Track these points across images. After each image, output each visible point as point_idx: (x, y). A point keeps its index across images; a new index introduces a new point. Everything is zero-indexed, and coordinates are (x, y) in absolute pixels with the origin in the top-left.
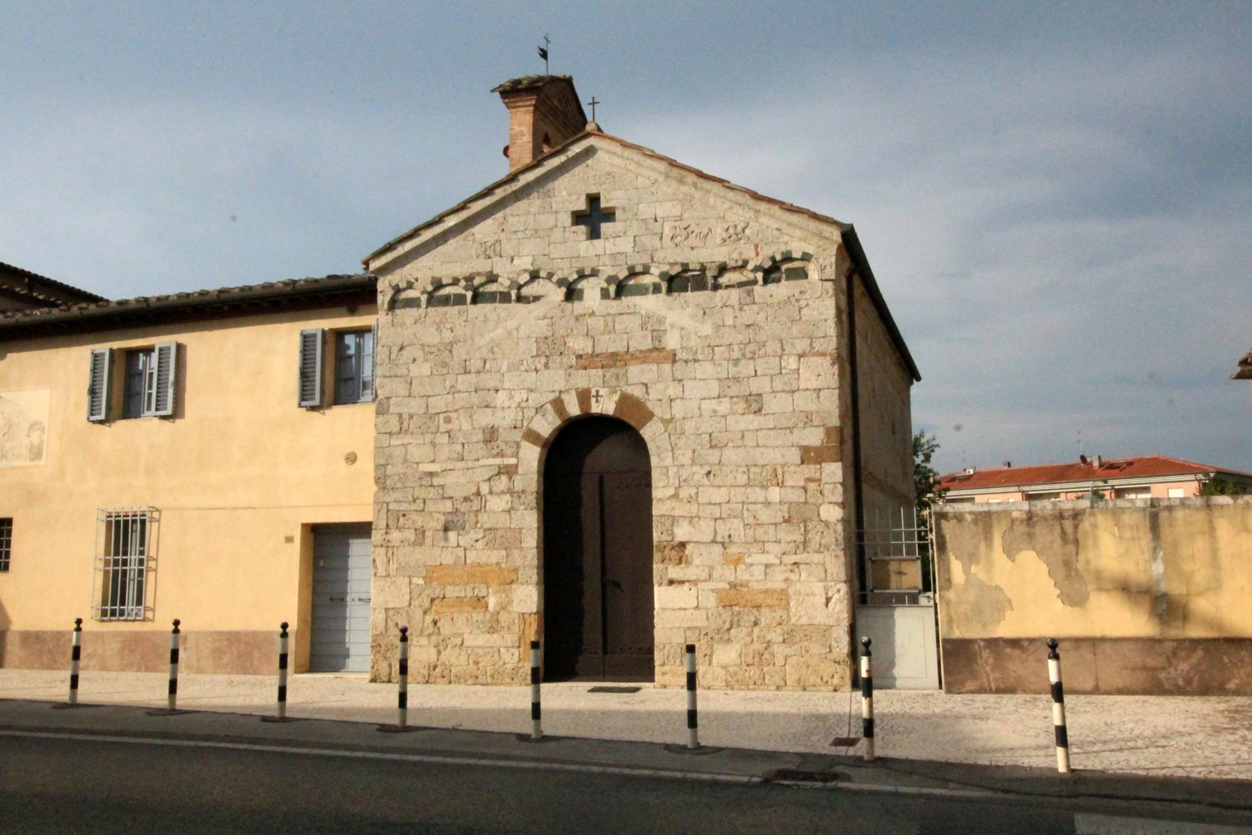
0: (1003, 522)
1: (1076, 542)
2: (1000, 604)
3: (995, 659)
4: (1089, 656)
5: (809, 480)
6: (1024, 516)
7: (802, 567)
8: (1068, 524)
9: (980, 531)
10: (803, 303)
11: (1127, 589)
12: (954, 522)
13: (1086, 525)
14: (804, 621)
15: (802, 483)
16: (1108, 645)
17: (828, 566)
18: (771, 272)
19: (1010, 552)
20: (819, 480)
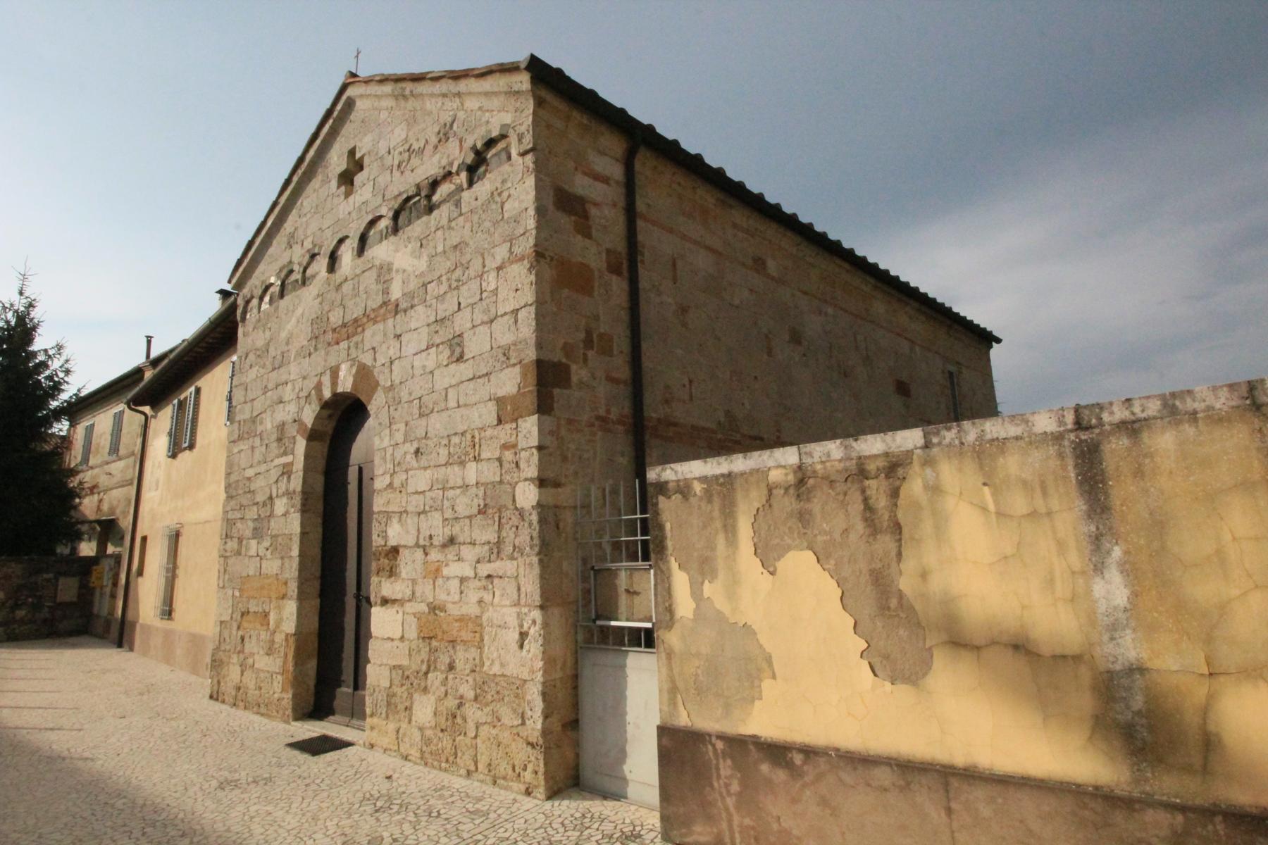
0: (754, 494)
1: (897, 528)
2: (751, 668)
3: (744, 784)
4: (936, 815)
5: (505, 447)
6: (791, 478)
7: (496, 581)
8: (877, 489)
9: (716, 513)
10: (505, 194)
11: (1020, 659)
12: (677, 498)
13: (915, 487)
14: (496, 669)
15: (497, 455)
16: (979, 793)
17: (522, 581)
18: (476, 166)
19: (767, 555)
20: (514, 446)
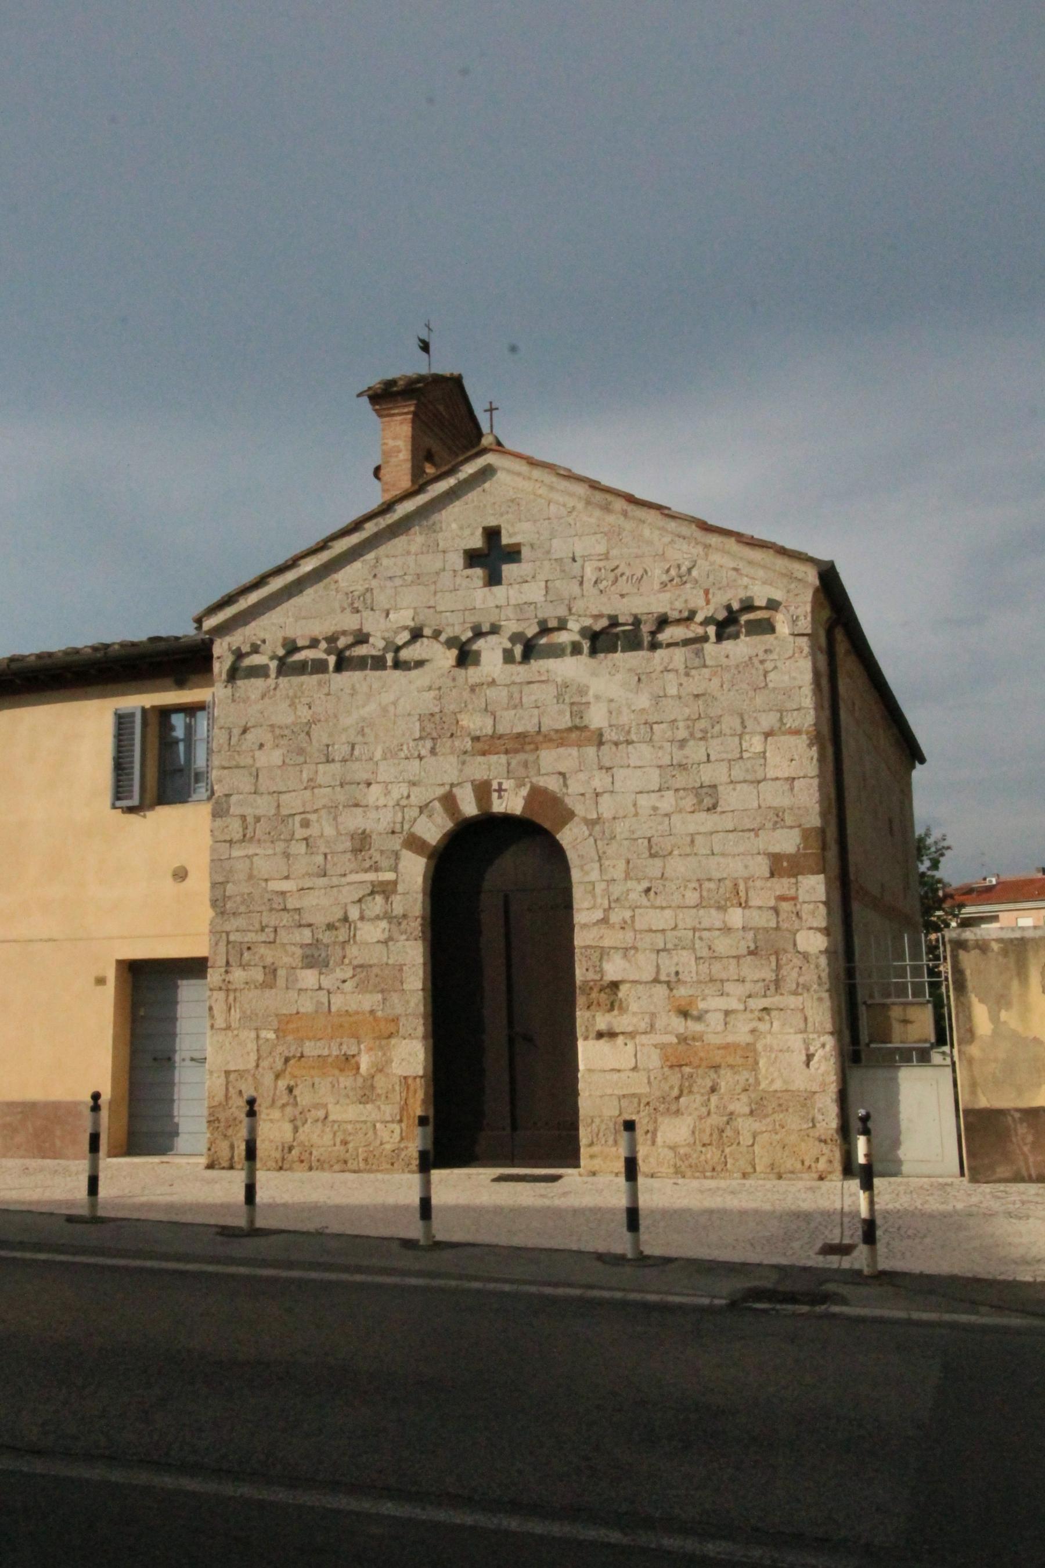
5: (782, 898)
7: (774, 1013)
9: (1012, 965)
10: (769, 665)
14: (778, 1085)
15: (772, 903)
17: (809, 1013)
20: (794, 899)
